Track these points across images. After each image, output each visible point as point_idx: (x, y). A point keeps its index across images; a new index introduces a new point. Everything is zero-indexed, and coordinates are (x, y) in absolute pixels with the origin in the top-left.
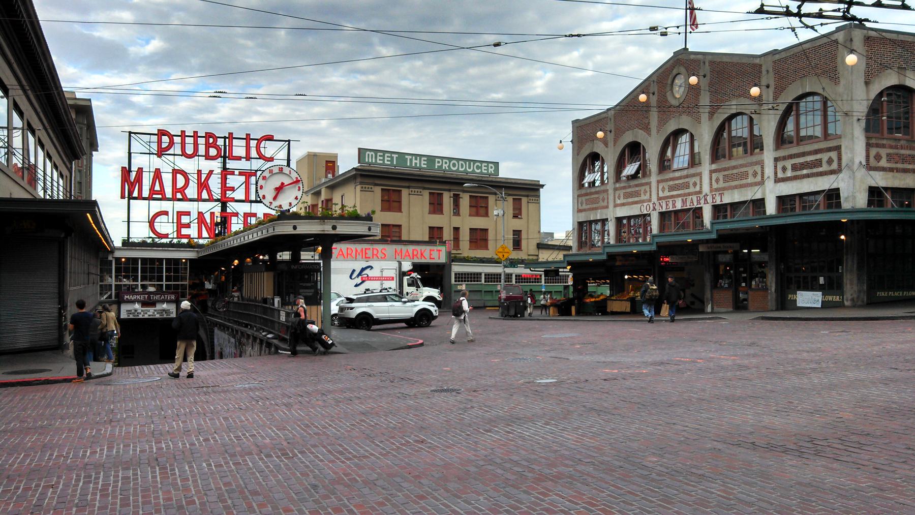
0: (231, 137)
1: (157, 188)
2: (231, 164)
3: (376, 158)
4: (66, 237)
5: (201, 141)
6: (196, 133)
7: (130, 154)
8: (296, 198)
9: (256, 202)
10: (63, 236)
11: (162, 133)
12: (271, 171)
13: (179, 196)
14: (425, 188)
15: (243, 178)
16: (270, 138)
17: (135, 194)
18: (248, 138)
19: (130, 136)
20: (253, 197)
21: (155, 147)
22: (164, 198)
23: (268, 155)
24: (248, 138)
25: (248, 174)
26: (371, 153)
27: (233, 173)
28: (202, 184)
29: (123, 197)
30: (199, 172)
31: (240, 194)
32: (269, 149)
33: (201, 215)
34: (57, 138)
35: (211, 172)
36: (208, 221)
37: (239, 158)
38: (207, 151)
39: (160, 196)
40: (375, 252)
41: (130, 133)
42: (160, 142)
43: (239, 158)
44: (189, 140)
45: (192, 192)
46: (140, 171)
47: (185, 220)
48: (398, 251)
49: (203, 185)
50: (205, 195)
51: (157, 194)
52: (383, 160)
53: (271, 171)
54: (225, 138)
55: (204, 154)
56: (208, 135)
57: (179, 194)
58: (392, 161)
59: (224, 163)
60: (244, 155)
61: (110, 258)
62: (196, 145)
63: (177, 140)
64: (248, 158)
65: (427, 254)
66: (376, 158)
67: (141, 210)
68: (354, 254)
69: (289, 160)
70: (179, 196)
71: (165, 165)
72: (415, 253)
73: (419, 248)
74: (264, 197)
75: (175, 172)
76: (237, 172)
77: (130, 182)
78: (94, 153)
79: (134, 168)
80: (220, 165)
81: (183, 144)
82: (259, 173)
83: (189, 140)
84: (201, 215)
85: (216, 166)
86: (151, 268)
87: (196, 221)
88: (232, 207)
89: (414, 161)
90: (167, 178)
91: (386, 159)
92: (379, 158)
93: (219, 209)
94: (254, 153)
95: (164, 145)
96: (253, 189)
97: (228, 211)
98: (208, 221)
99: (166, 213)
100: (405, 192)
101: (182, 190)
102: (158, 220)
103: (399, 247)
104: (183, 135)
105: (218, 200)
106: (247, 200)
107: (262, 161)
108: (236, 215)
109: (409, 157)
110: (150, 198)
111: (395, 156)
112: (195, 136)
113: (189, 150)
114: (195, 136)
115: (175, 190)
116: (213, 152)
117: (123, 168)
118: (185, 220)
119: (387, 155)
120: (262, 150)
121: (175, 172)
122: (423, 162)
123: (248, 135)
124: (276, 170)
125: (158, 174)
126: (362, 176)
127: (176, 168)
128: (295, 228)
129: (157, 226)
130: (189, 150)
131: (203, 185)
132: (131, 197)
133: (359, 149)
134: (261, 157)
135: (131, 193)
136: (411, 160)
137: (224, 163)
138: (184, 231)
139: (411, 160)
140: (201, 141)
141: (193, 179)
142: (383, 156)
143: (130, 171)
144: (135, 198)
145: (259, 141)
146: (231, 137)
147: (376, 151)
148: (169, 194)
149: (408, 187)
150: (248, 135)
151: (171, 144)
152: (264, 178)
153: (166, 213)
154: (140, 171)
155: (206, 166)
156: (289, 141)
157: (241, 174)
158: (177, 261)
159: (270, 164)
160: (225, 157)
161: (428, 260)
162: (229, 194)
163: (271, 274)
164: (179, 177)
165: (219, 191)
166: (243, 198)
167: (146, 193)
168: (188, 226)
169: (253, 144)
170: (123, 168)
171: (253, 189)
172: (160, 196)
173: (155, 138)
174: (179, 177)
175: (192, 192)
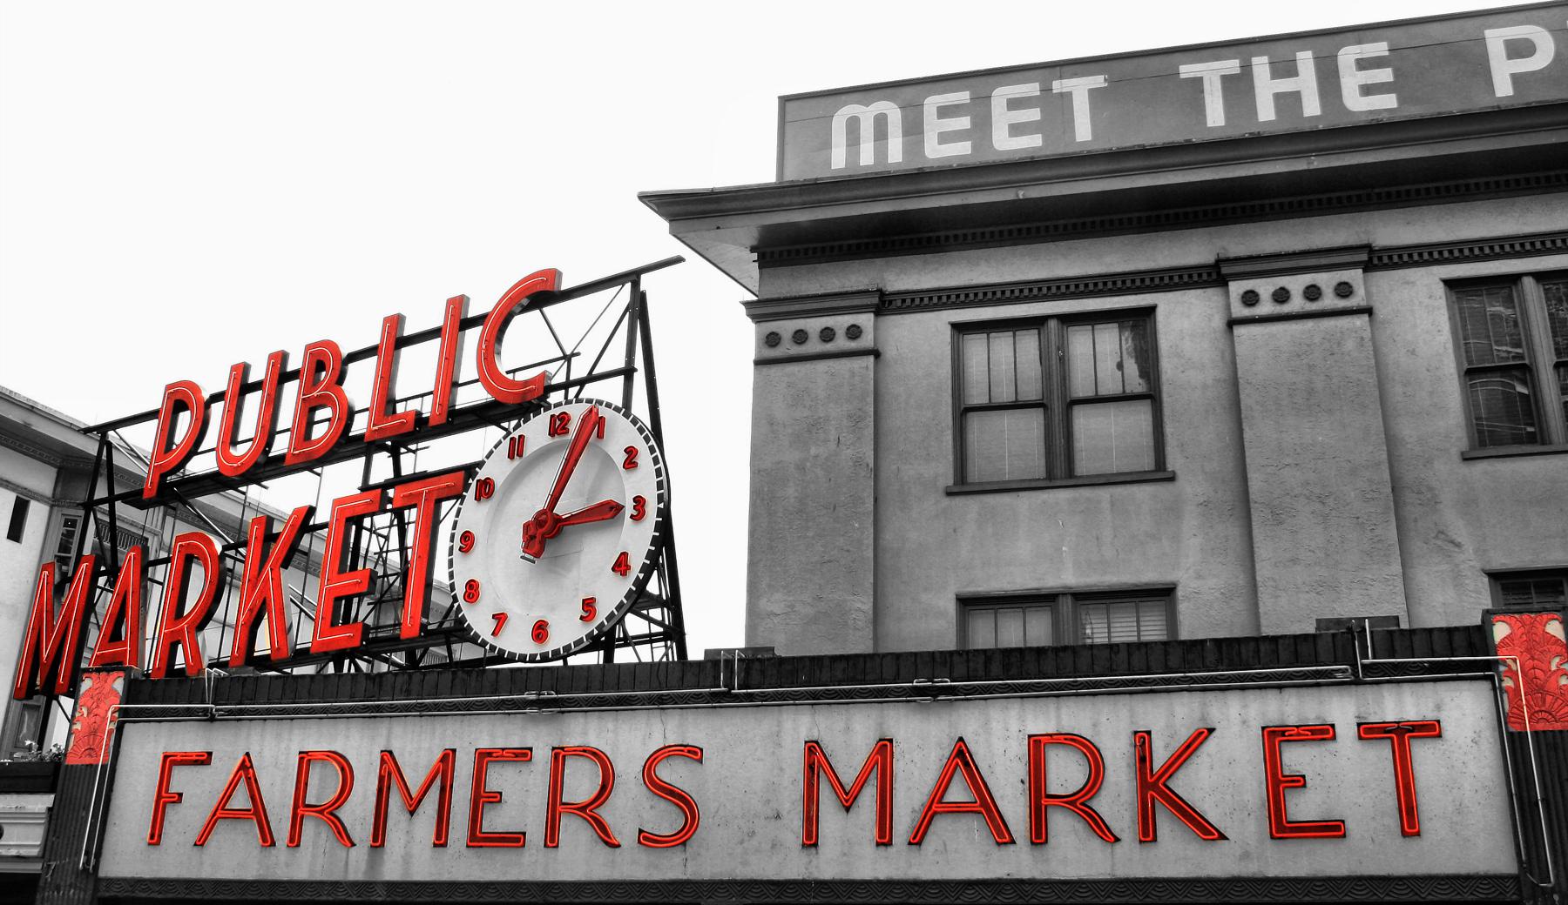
3: (913, 129)
8: (621, 566)
14: (1377, 260)
26: (865, 114)
40: (580, 783)
48: (849, 758)
65: (1224, 778)
66: (913, 129)
68: (358, 812)
72: (1065, 773)
73: (1109, 722)
74: (472, 590)
89: (1266, 87)
91: (1001, 117)
92: (933, 126)
100: (1185, 320)
103: (849, 733)
109: (1212, 73)
111: (1080, 88)
119: (1002, 94)
122: (1351, 81)
133: (785, 101)
136: (1238, 88)
139: (1238, 88)
149: (1214, 276)
156: (633, 277)
161: (1247, 853)
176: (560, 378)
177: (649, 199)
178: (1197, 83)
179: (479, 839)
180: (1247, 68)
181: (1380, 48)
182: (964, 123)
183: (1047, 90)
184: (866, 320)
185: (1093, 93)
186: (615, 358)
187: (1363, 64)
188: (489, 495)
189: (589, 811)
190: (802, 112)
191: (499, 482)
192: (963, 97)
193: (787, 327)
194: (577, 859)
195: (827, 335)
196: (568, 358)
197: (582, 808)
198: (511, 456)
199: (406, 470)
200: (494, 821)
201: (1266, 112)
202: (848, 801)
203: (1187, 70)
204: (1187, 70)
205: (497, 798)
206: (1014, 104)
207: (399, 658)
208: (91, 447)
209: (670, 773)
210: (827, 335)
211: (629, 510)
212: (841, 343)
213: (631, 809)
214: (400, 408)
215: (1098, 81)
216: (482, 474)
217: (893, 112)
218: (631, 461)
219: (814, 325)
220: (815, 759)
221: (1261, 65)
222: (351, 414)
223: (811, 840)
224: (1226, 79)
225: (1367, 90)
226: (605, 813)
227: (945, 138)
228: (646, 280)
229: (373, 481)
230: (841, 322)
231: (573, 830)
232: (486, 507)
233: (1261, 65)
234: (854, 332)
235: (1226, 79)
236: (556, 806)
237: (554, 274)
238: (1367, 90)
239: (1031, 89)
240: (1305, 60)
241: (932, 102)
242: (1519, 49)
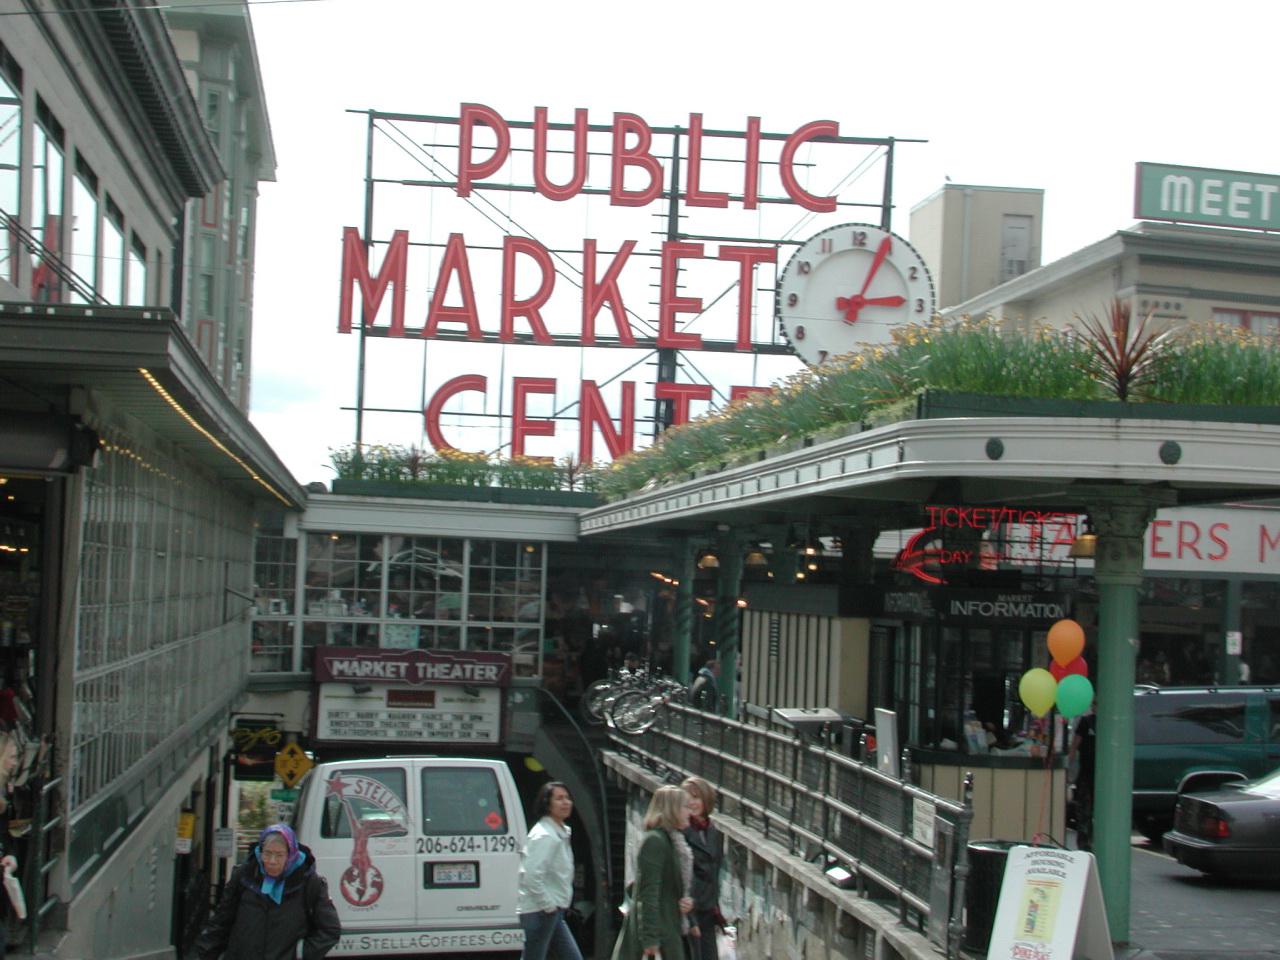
0: (696, 129)
1: (453, 298)
2: (695, 221)
4: (72, 467)
5: (599, 143)
6: (581, 114)
7: (370, 183)
9: (773, 349)
10: (59, 459)
11: (475, 115)
12: (827, 247)
13: (522, 325)
15: (733, 269)
16: (824, 132)
17: (383, 318)
18: (753, 133)
19: (371, 125)
20: (763, 330)
21: (449, 164)
22: (475, 335)
23: (816, 188)
24: (753, 133)
25: (748, 255)
27: (697, 252)
28: (596, 289)
29: (345, 326)
30: (590, 249)
31: (719, 323)
32: (819, 167)
33: (590, 390)
34: (123, 112)
35: (628, 248)
36: (614, 408)
37: (720, 200)
38: (617, 176)
39: (462, 327)
41: (373, 115)
42: (465, 146)
43: (720, 200)
44: (561, 141)
45: (563, 312)
46: (400, 243)
47: (538, 405)
49: (600, 293)
50: (605, 324)
51: (453, 320)
52: (1223, 205)
53: (827, 247)
54: (677, 132)
55: (606, 185)
56: (626, 123)
57: (523, 320)
58: (1254, 207)
59: (674, 217)
60: (738, 190)
61: (291, 532)
62: (581, 156)
63: (522, 139)
64: (751, 200)
67: (404, 371)
69: (887, 208)
70: (522, 325)
71: (481, 222)
74: (801, 333)
75: (514, 245)
76: (712, 249)
77: (368, 276)
78: (262, 186)
79: (382, 232)
80: (663, 225)
81: (540, 152)
82: (785, 253)
83: (561, 141)
84: (590, 390)
85: (647, 225)
86: (420, 570)
87: (574, 412)
88: (693, 366)
90: (486, 271)
91: (1235, 199)
92: (1206, 197)
93: (652, 373)
94: (770, 183)
95: (479, 157)
96: (763, 304)
97: (681, 378)
98: (614, 408)
99: (477, 383)
101: (531, 309)
102: (452, 404)
104: (541, 123)
105: (646, 343)
106: (744, 344)
107: (797, 210)
108: (705, 392)
110: (429, 332)
112: (581, 125)
113: (560, 171)
114: (581, 125)
115: (511, 308)
116: (637, 179)
117: (350, 232)
118: (538, 405)
119: (1237, 186)
120: (799, 173)
121: (514, 245)
123: (754, 122)
124: (843, 241)
125: (456, 254)
126: (1145, 260)
127: (516, 232)
128: (995, 450)
129: (448, 427)
130: (560, 171)
131: (600, 293)
132: (369, 330)
133: (1143, 169)
134: (797, 196)
135: (369, 313)
137: (674, 217)
138: (535, 446)
140: (599, 143)
141: (570, 269)
142: (1224, 191)
143: (368, 242)
144: (382, 332)
145: (791, 142)
146: (696, 129)
147: (1198, 173)
148: (490, 321)
150: (754, 122)
151: (503, 150)
152: (804, 269)
153: (477, 383)
154: (400, 243)
155: (611, 225)
156: (890, 142)
157: (726, 254)
158: (508, 549)
159: (824, 220)
160: (674, 197)
162: (686, 323)
163: (860, 627)
164: (526, 264)
165: (654, 313)
166: (732, 336)
167: (416, 316)
168: (546, 428)
169: (770, 151)
170: (350, 232)
171: (763, 304)
172: (462, 327)
173: (452, 133)
174: (526, 264)
175: (563, 312)
179: (1155, 554)
182: (1217, 198)
183: (1253, 188)
184: (1181, 300)
188: (806, 273)
189: (1191, 546)
191: (814, 264)
192: (1218, 183)
193: (1151, 298)
194: (1188, 564)
197: (1191, 546)
198: (824, 251)
200: (1161, 548)
202: (1273, 546)
205: (1159, 539)
206: (1241, 193)
209: (1218, 533)
211: (914, 306)
212: (1172, 311)
213: (1206, 546)
216: (803, 258)
218: (913, 278)
219: (1162, 299)
220: (1264, 532)
222: (656, 171)
223: (1262, 559)
226: (1196, 546)
228: (896, 143)
230: (1173, 300)
231: (1187, 551)
232: (803, 279)
234: (1178, 306)
236: (1181, 544)
237: (835, 125)
239: (1246, 186)
241: (1208, 183)
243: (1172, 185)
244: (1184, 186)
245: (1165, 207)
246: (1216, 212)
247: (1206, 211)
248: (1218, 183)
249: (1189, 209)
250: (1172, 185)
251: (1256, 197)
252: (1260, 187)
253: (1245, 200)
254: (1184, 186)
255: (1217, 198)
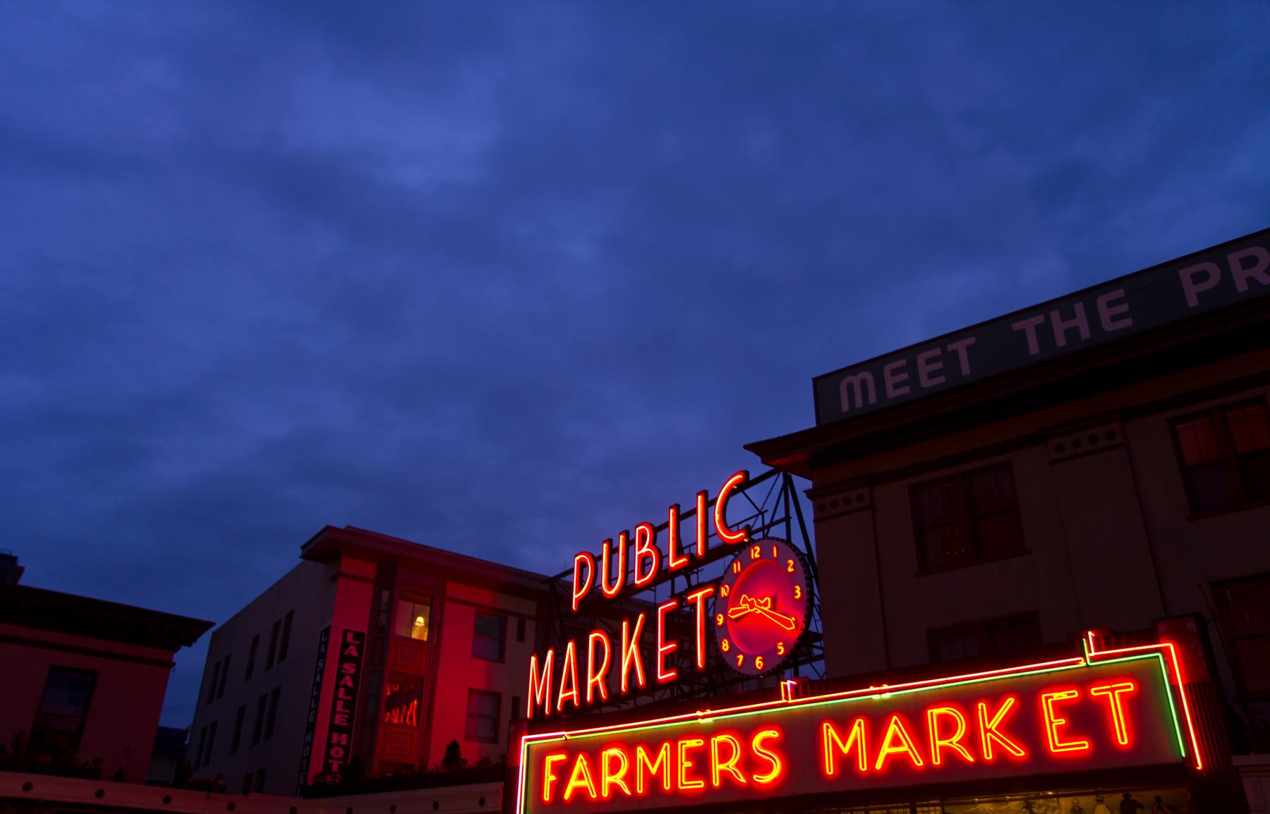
3: (880, 384)
26: (855, 380)
52: (914, 379)
66: (880, 384)
91: (924, 370)
92: (890, 381)
109: (1029, 325)
111: (961, 347)
119: (922, 357)
122: (1105, 313)
133: (815, 380)
136: (1045, 332)
139: (1045, 332)
142: (912, 368)
176: (758, 525)
177: (753, 447)
178: (1023, 332)
180: (1048, 318)
181: (1119, 293)
182: (904, 376)
185: (968, 348)
186: (780, 514)
187: (1111, 304)
190: (825, 386)
192: (903, 362)
195: (847, 501)
196: (761, 513)
199: (694, 582)
201: (1061, 341)
203: (1016, 326)
204: (1016, 326)
207: (705, 680)
208: (546, 587)
210: (847, 501)
214: (686, 551)
215: (972, 341)
217: (868, 376)
221: (1055, 315)
224: (1037, 327)
225: (1114, 318)
227: (896, 386)
229: (677, 591)
233: (1055, 315)
235: (1037, 327)
238: (1114, 318)
239: (937, 352)
240: (1079, 308)
241: (888, 368)
242: (1200, 277)
243: (850, 387)
244: (864, 383)
245: (845, 407)
246: (906, 390)
247: (892, 393)
248: (903, 362)
249: (873, 399)
250: (850, 387)
251: (951, 359)
252: (950, 347)
253: (939, 365)
254: (864, 383)
255: (904, 376)
